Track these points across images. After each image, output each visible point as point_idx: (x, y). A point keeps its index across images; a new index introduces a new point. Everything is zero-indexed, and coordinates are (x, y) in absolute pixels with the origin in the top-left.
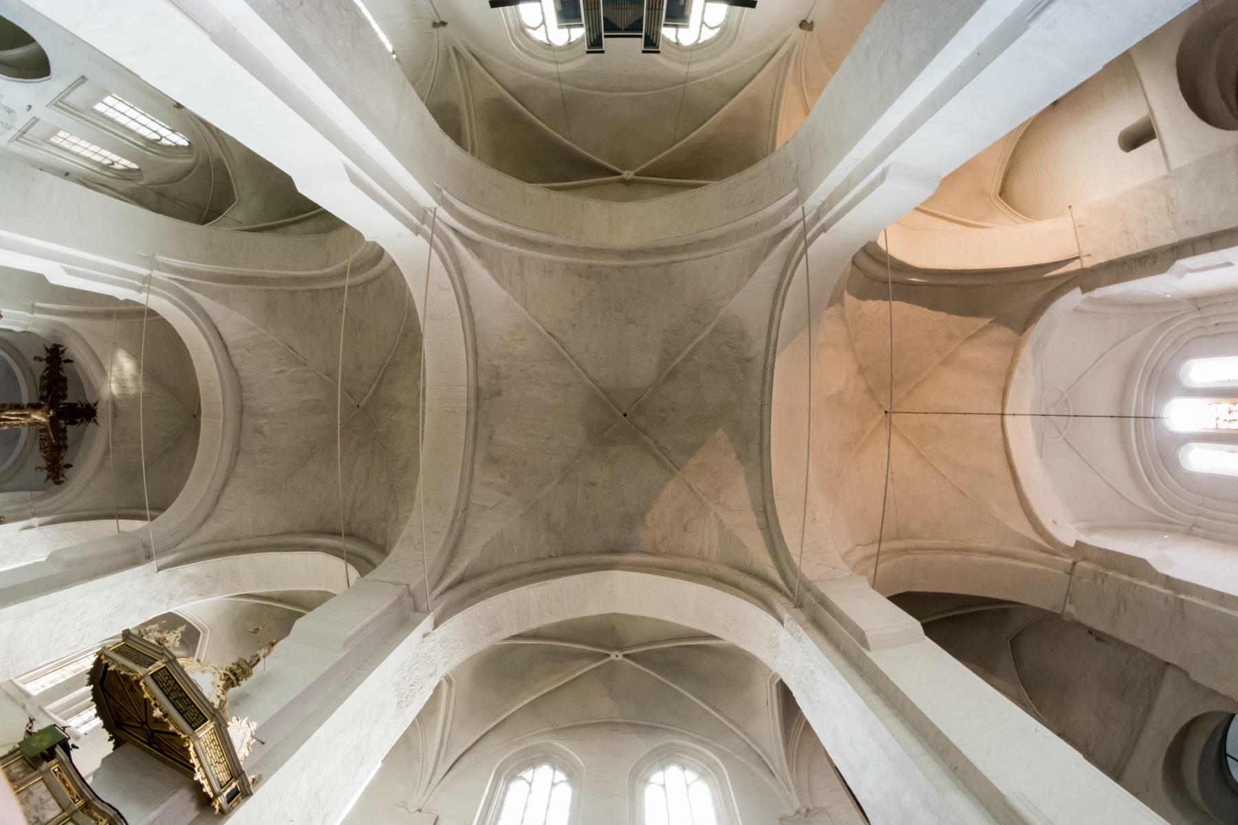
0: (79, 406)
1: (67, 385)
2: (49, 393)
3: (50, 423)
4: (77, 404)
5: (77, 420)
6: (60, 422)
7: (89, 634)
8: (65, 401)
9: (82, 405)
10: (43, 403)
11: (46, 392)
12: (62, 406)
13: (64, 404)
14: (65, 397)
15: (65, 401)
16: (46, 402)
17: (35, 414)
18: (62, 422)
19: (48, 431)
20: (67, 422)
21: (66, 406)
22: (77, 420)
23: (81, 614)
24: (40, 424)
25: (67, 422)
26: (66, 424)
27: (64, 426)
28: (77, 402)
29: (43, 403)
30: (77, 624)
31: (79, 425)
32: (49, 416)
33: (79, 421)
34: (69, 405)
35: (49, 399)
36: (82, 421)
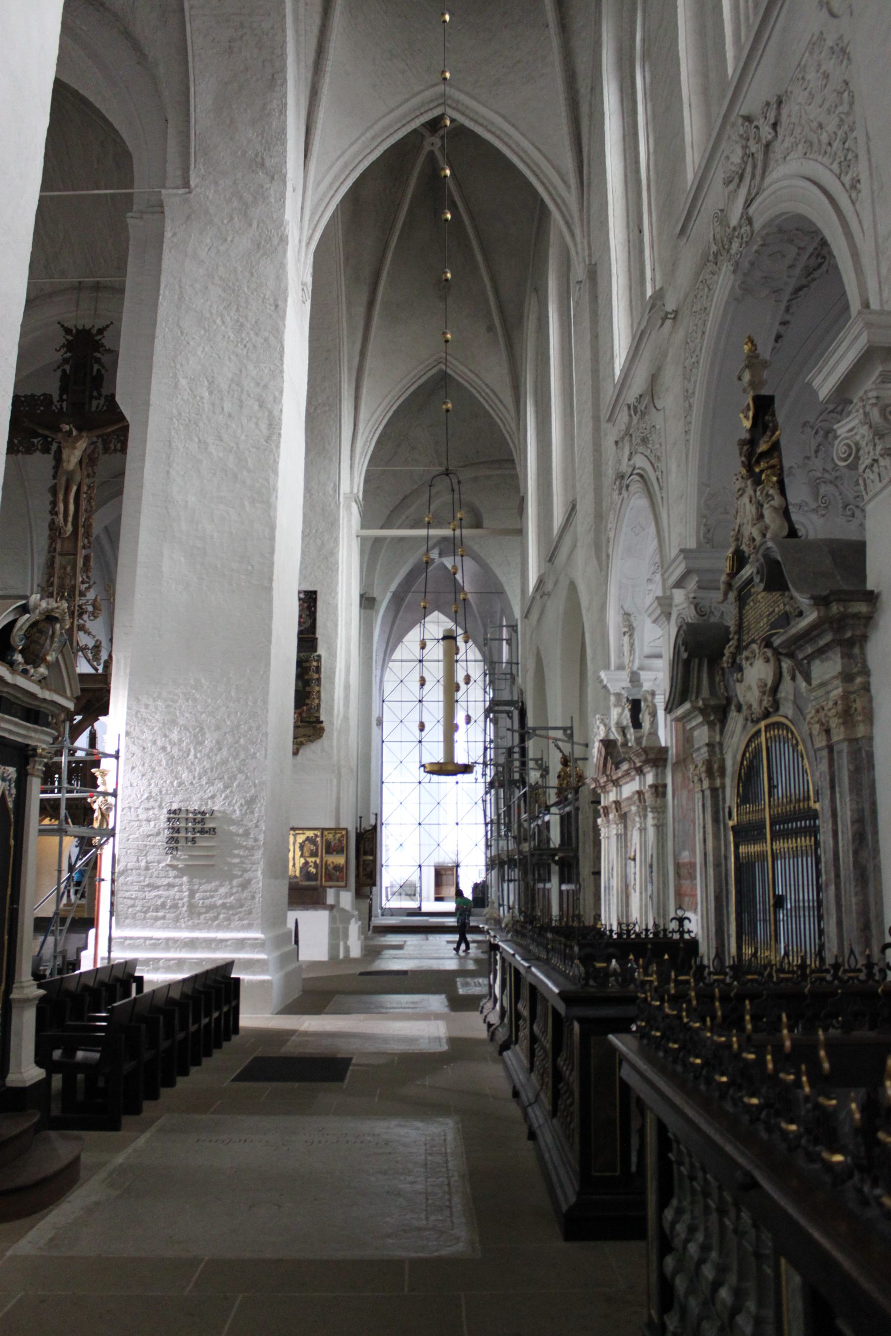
0: (67, 368)
1: (25, 396)
2: (36, 435)
3: (90, 429)
4: (64, 371)
5: (95, 372)
6: (94, 409)
7: (258, 384)
8: (56, 398)
9: (65, 361)
10: (54, 447)
11: (35, 441)
12: (65, 404)
13: (61, 400)
14: (47, 397)
15: (56, 398)
16: (53, 439)
17: (69, 461)
18: (94, 403)
19: (109, 434)
20: (95, 394)
21: (65, 397)
22: (95, 372)
23: (211, 393)
24: (93, 452)
25: (95, 394)
26: (100, 395)
27: (102, 401)
28: (59, 373)
29: (54, 447)
30: (227, 406)
31: (103, 367)
32: (75, 433)
33: (96, 367)
34: (64, 389)
35: (46, 433)
36: (98, 361)
